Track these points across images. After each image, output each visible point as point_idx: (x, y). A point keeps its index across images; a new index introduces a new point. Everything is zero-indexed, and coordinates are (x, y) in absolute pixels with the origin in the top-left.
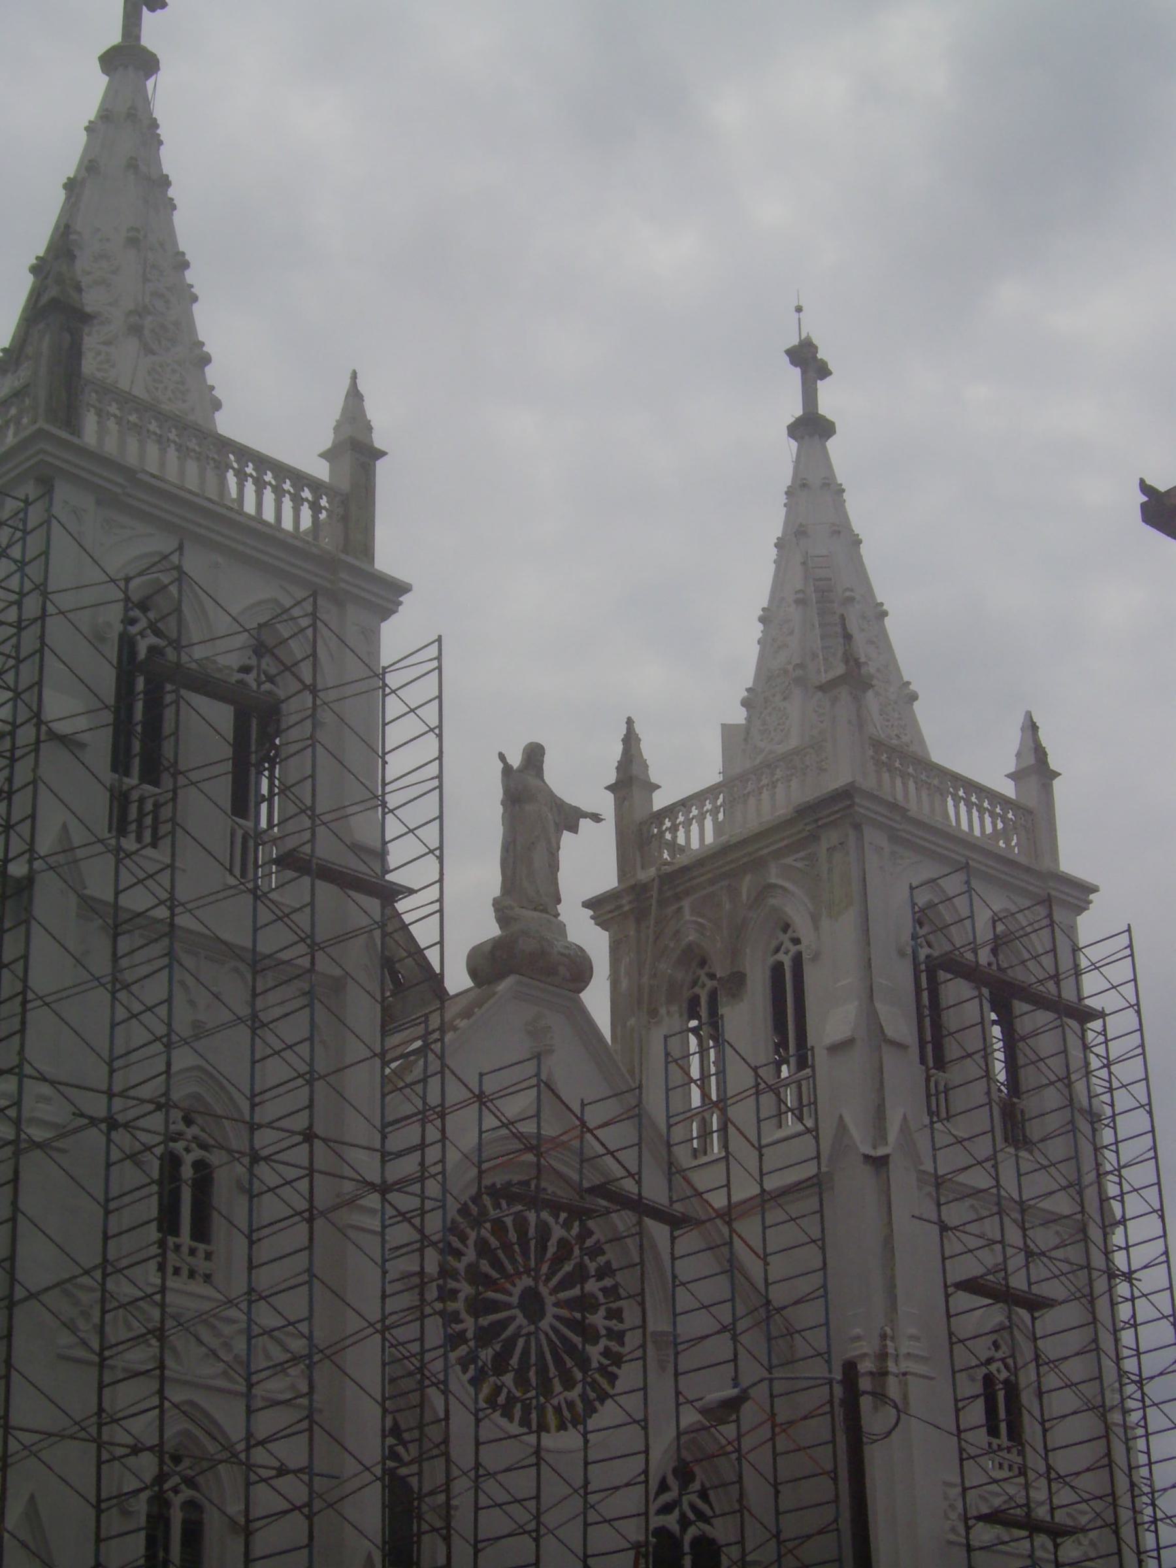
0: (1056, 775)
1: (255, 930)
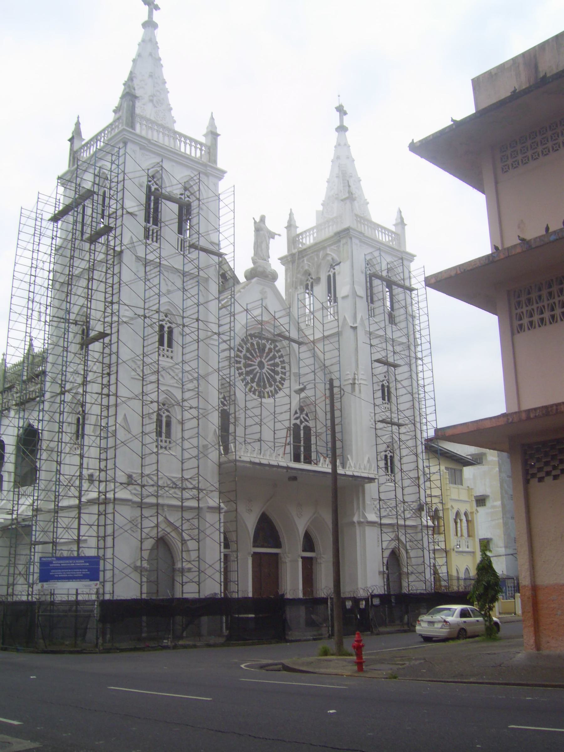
1: (184, 265)
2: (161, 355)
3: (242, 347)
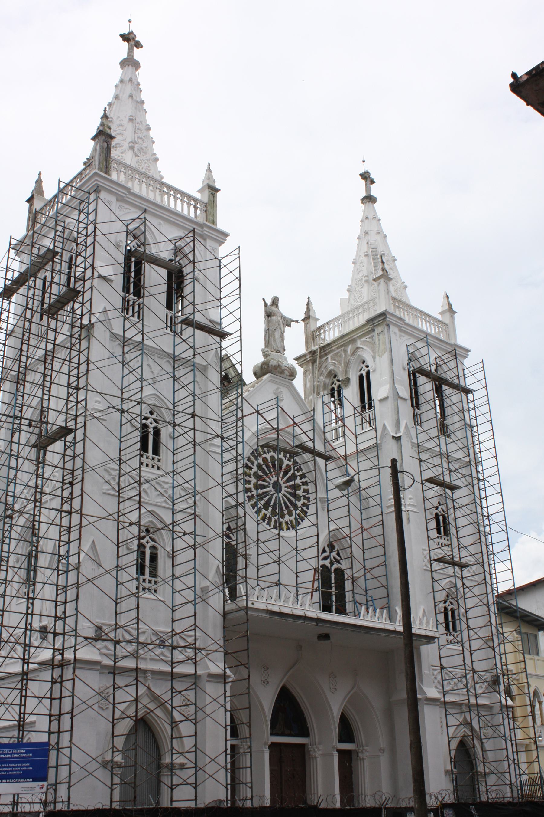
0: (456, 312)
1: (175, 346)
2: (145, 464)
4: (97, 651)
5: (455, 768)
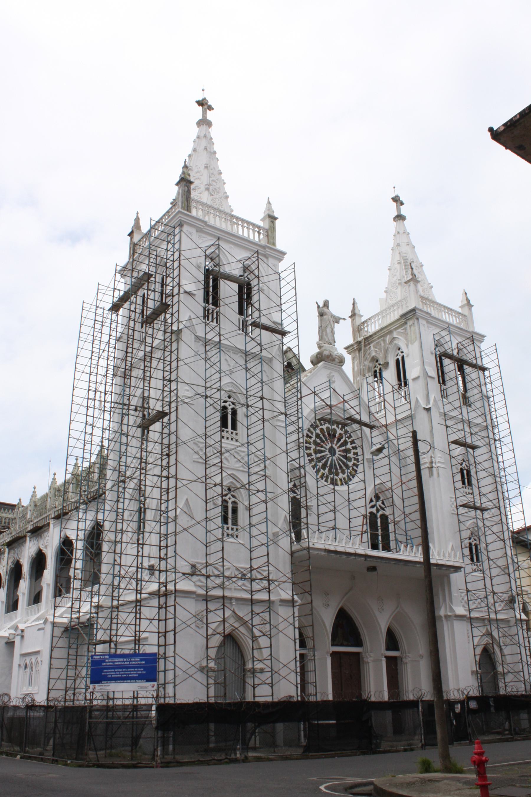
0: (473, 306)
1: (246, 344)
2: (225, 438)
3: (312, 433)
4: (193, 584)
5: (480, 669)
